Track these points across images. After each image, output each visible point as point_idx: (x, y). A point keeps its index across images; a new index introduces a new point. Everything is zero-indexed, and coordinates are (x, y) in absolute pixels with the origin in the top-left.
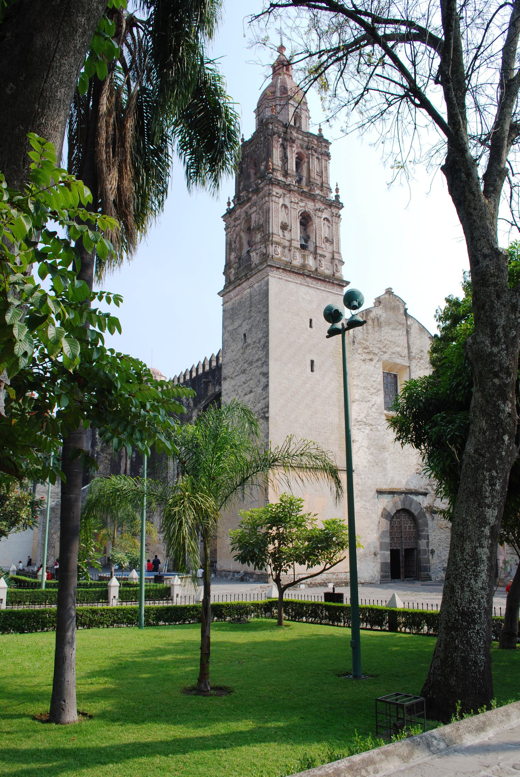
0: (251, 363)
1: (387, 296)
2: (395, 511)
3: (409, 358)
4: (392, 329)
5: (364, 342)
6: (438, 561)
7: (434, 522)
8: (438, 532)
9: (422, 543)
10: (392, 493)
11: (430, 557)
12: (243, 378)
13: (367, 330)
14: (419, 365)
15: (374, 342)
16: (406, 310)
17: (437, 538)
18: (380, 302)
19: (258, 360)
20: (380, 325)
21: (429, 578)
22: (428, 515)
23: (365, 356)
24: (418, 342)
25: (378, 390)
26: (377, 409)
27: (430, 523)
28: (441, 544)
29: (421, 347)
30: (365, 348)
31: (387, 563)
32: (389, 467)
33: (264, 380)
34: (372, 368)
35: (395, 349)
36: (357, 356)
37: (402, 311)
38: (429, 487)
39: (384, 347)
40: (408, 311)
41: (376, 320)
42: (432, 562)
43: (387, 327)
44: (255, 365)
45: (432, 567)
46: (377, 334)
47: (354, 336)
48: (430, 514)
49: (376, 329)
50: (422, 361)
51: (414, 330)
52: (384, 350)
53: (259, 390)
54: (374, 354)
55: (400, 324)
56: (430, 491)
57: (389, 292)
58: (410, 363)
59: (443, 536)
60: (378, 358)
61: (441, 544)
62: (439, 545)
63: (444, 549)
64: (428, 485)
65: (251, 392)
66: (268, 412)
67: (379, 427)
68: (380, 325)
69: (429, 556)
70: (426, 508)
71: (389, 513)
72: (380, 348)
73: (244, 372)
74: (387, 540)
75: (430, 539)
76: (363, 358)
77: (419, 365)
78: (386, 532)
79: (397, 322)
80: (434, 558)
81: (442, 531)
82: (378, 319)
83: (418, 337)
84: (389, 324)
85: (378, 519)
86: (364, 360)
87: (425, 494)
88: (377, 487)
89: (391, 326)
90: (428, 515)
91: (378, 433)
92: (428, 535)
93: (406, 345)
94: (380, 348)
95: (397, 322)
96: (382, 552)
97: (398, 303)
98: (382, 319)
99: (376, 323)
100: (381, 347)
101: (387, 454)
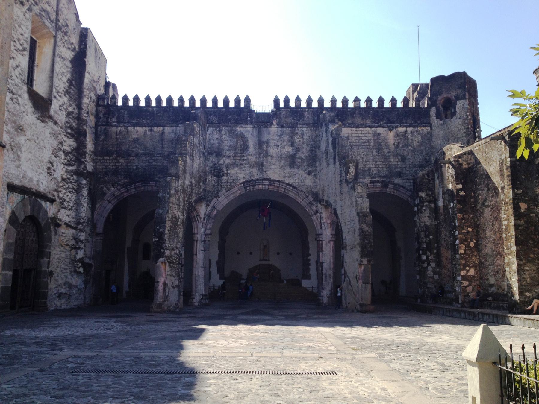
3: (56, 26)
8: (58, 249)
10: (23, 190)
11: (49, 281)
14: (64, 40)
25: (24, 49)
26: (20, 74)
28: (60, 265)
32: (24, 156)
38: (55, 193)
45: (49, 293)
48: (54, 227)
50: (66, 38)
56: (57, 198)
58: (56, 33)
59: (63, 255)
61: (60, 265)
62: (57, 266)
63: (61, 271)
67: (19, 99)
74: (11, 256)
81: (62, 248)
83: (66, 6)
87: (52, 201)
88: (8, 180)
90: (52, 227)
91: (18, 107)
93: (55, 8)
96: (4, 272)
101: (22, 139)
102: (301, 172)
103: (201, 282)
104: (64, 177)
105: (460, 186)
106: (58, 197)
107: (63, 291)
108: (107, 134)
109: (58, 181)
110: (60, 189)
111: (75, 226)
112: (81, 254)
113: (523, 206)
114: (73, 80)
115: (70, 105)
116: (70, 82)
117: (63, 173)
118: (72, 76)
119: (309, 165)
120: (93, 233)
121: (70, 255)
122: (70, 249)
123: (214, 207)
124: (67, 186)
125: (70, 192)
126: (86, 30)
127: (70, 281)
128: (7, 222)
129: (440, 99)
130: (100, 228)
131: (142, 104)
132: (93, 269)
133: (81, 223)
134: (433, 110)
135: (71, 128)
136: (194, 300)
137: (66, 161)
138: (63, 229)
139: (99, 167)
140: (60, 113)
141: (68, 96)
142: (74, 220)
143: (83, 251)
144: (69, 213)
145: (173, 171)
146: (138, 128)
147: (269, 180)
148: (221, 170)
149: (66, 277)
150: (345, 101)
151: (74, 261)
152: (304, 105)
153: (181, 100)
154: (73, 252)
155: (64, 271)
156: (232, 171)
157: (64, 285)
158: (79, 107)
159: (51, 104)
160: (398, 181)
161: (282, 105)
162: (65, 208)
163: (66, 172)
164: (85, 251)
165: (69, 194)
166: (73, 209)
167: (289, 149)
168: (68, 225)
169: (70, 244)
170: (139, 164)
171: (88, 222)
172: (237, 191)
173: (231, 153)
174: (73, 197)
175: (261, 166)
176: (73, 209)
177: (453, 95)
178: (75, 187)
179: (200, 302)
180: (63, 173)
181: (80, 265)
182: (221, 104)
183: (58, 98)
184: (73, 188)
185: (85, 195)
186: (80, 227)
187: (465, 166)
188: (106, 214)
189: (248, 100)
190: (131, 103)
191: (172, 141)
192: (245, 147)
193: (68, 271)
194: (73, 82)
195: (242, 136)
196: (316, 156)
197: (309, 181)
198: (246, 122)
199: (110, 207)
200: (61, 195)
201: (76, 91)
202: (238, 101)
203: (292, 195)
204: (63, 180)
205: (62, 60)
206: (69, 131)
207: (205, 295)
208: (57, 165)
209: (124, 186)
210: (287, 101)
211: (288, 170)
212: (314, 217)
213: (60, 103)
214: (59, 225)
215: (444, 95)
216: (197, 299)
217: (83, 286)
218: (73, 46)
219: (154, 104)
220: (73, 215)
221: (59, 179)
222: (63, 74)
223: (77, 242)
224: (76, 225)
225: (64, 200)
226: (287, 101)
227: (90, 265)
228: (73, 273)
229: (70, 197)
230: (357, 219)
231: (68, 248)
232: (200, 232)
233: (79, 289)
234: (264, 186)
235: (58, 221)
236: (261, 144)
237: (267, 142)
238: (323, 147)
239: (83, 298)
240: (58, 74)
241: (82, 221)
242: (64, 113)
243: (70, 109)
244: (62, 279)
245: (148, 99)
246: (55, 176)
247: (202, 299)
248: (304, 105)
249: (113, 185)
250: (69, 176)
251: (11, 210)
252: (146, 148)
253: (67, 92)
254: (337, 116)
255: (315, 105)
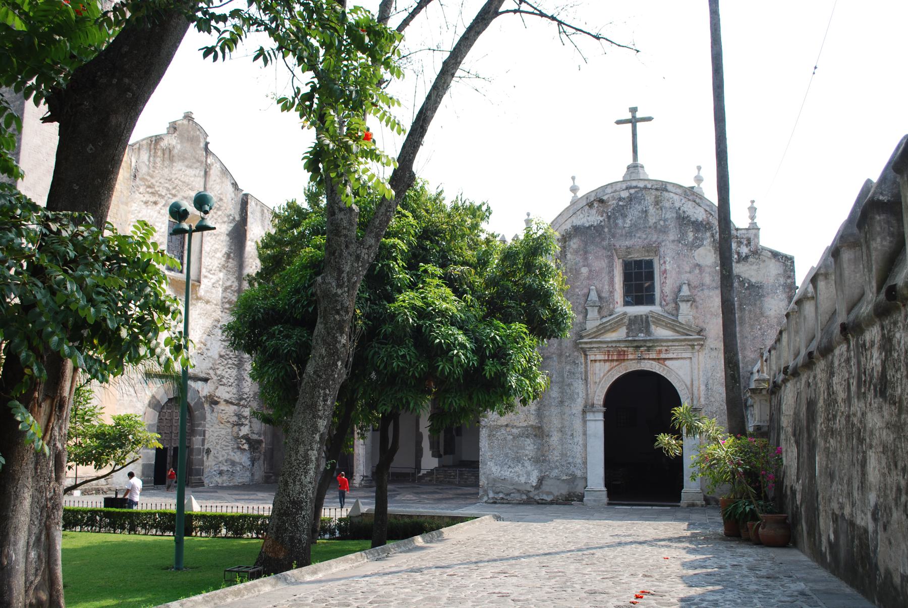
1: (185, 122)
2: (166, 400)
4: (187, 166)
5: (148, 178)
6: (214, 463)
7: (214, 414)
8: (217, 427)
9: (197, 440)
11: (205, 458)
13: (155, 163)
15: (162, 181)
16: (207, 144)
17: (216, 435)
18: (175, 129)
20: (171, 159)
21: (201, 484)
22: (206, 406)
23: (147, 197)
24: (218, 187)
27: (208, 416)
28: (220, 442)
29: (221, 194)
30: (149, 187)
31: (151, 465)
34: (156, 214)
35: (187, 193)
36: (137, 195)
37: (202, 145)
38: (211, 372)
39: (174, 188)
40: (209, 146)
41: (168, 150)
42: (206, 464)
43: (180, 163)
45: (206, 470)
46: (166, 170)
47: (136, 170)
48: (210, 405)
49: (167, 163)
50: (220, 213)
51: (215, 171)
52: (174, 192)
54: (160, 195)
55: (198, 161)
56: (213, 376)
57: (188, 117)
59: (223, 432)
60: (164, 202)
61: (220, 442)
62: (217, 443)
63: (221, 448)
64: (211, 368)
68: (171, 159)
69: (203, 456)
70: (206, 397)
71: (159, 402)
72: (168, 189)
75: (207, 436)
76: (144, 199)
77: (215, 216)
78: (154, 425)
79: (195, 158)
80: (210, 459)
81: (222, 426)
82: (170, 151)
83: (218, 181)
84: (183, 159)
85: (143, 410)
86: (146, 203)
87: (206, 380)
89: (186, 163)
90: (206, 406)
92: (204, 431)
94: (168, 189)
95: (195, 158)
97: (198, 133)
98: (175, 151)
99: (167, 156)
100: (171, 188)
103: (361, 462)
104: (222, 353)
106: (216, 374)
107: (225, 468)
109: (214, 359)
110: (218, 366)
111: (237, 402)
112: (245, 431)
114: (231, 252)
115: (228, 279)
116: (228, 256)
117: (220, 350)
118: (230, 248)
121: (232, 432)
122: (231, 426)
124: (226, 362)
125: (229, 368)
126: (246, 195)
127: (233, 458)
128: (146, 405)
132: (264, 445)
133: (245, 399)
135: (230, 302)
136: (355, 482)
137: (224, 337)
138: (222, 406)
140: (214, 290)
141: (225, 271)
142: (236, 396)
143: (247, 427)
144: (228, 389)
149: (228, 454)
151: (237, 438)
154: (236, 429)
155: (225, 448)
157: (226, 462)
159: (200, 286)
162: (224, 385)
163: (224, 348)
164: (251, 427)
165: (228, 370)
166: (234, 384)
168: (227, 402)
169: (231, 420)
171: (254, 397)
174: (234, 372)
176: (234, 384)
178: (236, 363)
179: (360, 484)
180: (221, 349)
181: (244, 441)
183: (211, 276)
184: (234, 364)
185: (248, 369)
186: (242, 403)
193: (229, 448)
194: (232, 255)
200: (219, 372)
201: (235, 263)
204: (221, 356)
205: (214, 237)
206: (227, 306)
207: (366, 477)
208: (212, 344)
213: (213, 281)
214: (217, 403)
217: (249, 463)
218: (231, 218)
220: (235, 391)
221: (217, 357)
222: (216, 251)
223: (239, 419)
224: (239, 401)
225: (223, 377)
227: (259, 442)
228: (235, 450)
229: (230, 374)
231: (229, 425)
233: (244, 467)
235: (216, 399)
239: (250, 475)
240: (209, 253)
241: (245, 396)
242: (220, 289)
243: (229, 283)
244: (223, 456)
246: (209, 354)
247: (363, 480)
250: (228, 352)
251: (151, 395)
253: (224, 267)
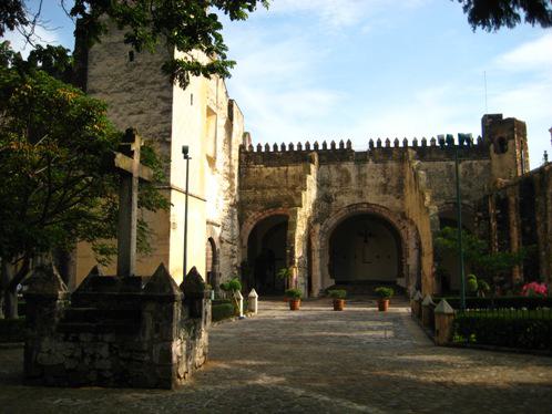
0: (142, 84)
12: (128, 96)
19: (154, 83)
33: (163, 105)
44: (147, 87)
53: (157, 113)
65: (141, 112)
66: (170, 136)
73: (130, 90)
102: (392, 197)
105: (498, 212)
108: (247, 174)
113: (528, 229)
119: (398, 191)
120: (242, 247)
123: (327, 226)
129: (497, 137)
130: (245, 243)
131: (272, 150)
134: (492, 147)
139: (244, 198)
145: (297, 202)
146: (269, 168)
147: (368, 203)
148: (331, 197)
150: (424, 141)
151: (232, 266)
152: (392, 145)
153: (299, 146)
156: (339, 198)
158: (230, 157)
160: (466, 202)
161: (375, 146)
167: (383, 180)
170: (271, 194)
172: (343, 213)
173: (338, 184)
175: (361, 194)
177: (505, 135)
182: (329, 147)
187: (502, 197)
188: (249, 232)
189: (349, 143)
190: (263, 150)
191: (294, 177)
192: (348, 179)
195: (346, 171)
196: (403, 184)
197: (397, 204)
198: (348, 160)
199: (252, 226)
202: (342, 144)
203: (385, 214)
209: (261, 211)
210: (379, 142)
211: (381, 196)
212: (402, 231)
215: (500, 135)
216: (316, 293)
219: (279, 149)
226: (379, 142)
230: (430, 234)
232: (316, 244)
234: (364, 208)
236: (360, 177)
237: (365, 175)
238: (408, 176)
245: (275, 146)
248: (392, 145)
249: (254, 211)
252: (275, 182)
254: (418, 153)
255: (401, 145)
